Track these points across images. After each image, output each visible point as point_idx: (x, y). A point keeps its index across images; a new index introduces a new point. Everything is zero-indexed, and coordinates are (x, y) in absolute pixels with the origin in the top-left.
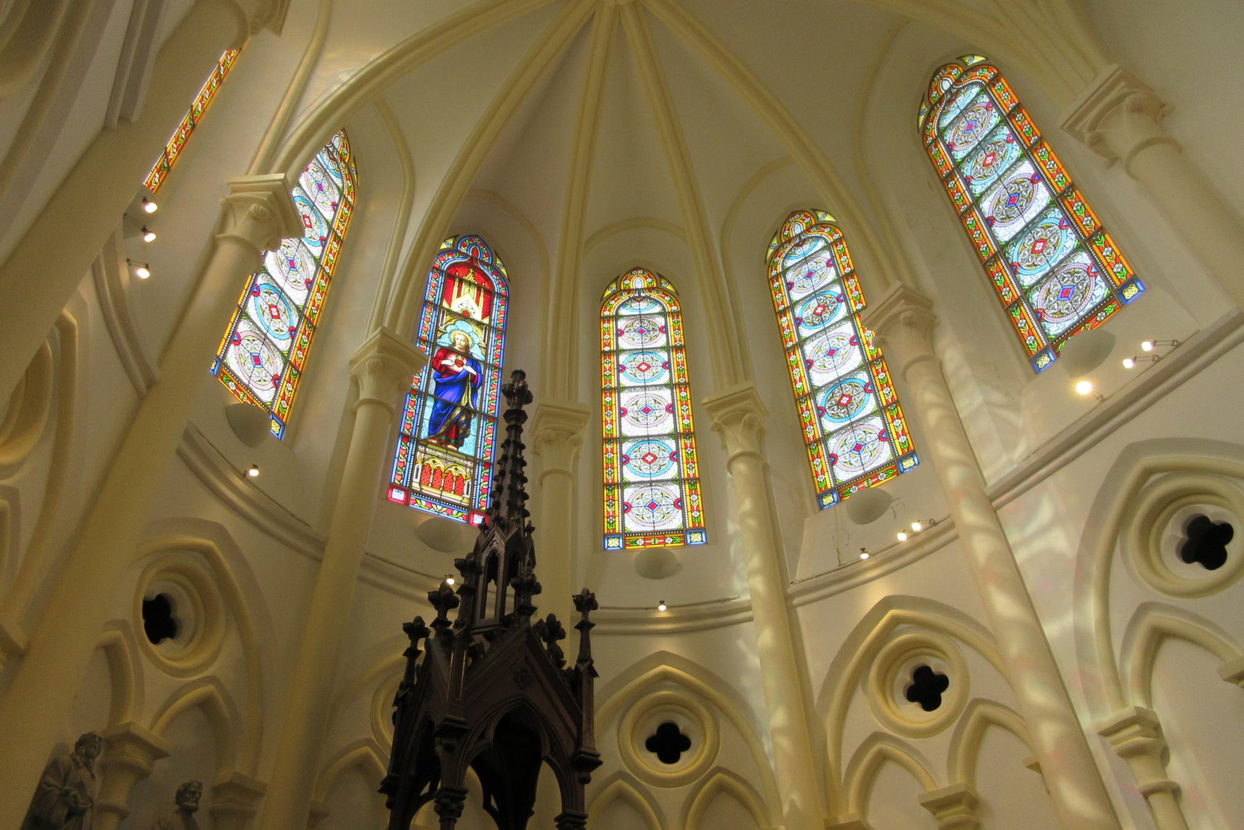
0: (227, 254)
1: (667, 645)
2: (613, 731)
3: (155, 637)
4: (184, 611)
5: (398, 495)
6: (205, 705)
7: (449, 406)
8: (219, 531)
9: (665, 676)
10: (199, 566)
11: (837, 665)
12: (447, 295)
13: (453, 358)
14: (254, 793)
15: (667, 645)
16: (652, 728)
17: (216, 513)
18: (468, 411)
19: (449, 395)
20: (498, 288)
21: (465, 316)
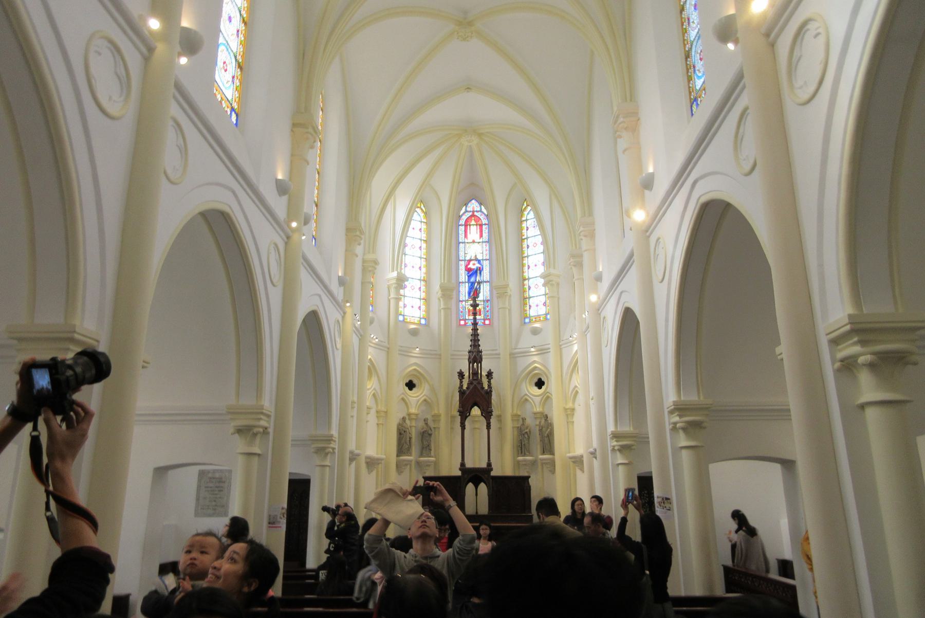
0: (392, 302)
1: (536, 358)
2: (524, 384)
3: (411, 389)
4: (415, 382)
5: (462, 323)
6: (425, 400)
7: (473, 284)
8: (415, 364)
9: (536, 367)
10: (415, 373)
11: (569, 366)
12: (466, 236)
13: (472, 263)
14: (440, 416)
15: (536, 358)
16: (536, 380)
17: (413, 361)
18: (479, 283)
19: (472, 279)
20: (485, 221)
21: (474, 242)
